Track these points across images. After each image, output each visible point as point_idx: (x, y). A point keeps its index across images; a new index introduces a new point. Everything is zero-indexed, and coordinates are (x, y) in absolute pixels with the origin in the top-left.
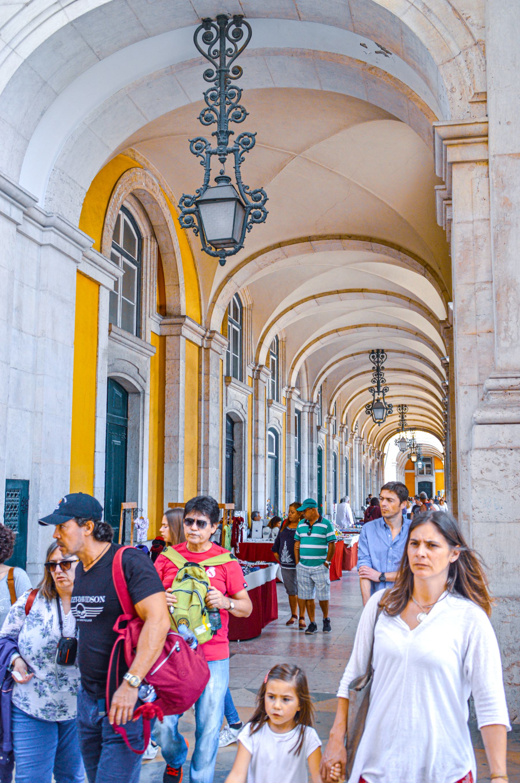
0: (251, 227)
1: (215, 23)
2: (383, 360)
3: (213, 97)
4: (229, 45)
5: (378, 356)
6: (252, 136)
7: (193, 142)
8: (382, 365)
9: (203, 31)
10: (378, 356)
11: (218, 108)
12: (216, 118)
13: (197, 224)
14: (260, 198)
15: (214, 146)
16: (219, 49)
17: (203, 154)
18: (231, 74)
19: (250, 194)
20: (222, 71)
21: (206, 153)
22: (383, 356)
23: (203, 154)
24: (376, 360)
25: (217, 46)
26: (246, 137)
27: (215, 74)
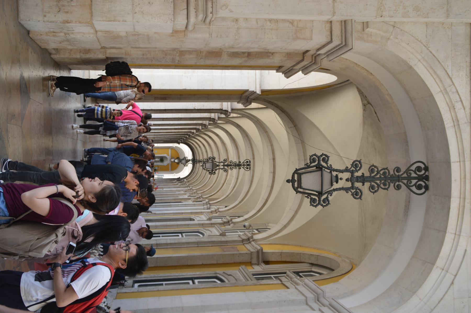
0: (308, 198)
1: (427, 174)
2: (245, 169)
3: (384, 173)
4: (414, 182)
5: (248, 165)
6: (360, 198)
7: (360, 162)
8: (242, 168)
9: (423, 166)
10: (248, 165)
11: (378, 176)
12: (373, 175)
13: (311, 165)
14: (325, 203)
15: (356, 174)
16: (412, 176)
17: (353, 168)
18: (397, 183)
19: (327, 198)
20: (399, 179)
21: (353, 170)
22: (247, 168)
23: (353, 168)
24: (245, 164)
25: (413, 175)
26: (360, 193)
27: (397, 174)
